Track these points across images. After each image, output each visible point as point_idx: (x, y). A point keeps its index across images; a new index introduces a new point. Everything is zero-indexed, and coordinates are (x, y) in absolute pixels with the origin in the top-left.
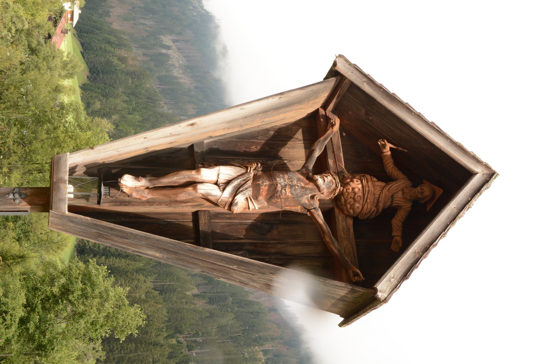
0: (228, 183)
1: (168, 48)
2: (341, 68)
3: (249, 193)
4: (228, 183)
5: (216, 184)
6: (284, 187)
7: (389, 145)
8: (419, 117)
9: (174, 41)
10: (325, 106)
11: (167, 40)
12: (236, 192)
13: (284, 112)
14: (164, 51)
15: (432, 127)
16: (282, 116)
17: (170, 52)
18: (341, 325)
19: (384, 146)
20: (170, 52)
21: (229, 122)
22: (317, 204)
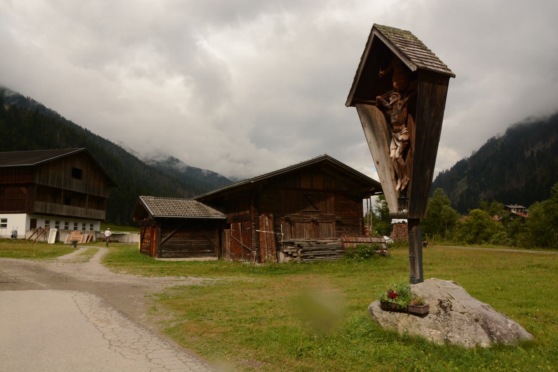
0: (396, 144)
1: (532, 152)
2: (348, 104)
3: (398, 134)
4: (396, 144)
5: (396, 149)
6: (394, 118)
7: (381, 72)
8: (360, 65)
9: (528, 150)
10: (373, 104)
11: (528, 154)
12: (398, 140)
13: (376, 121)
14: (535, 155)
15: (362, 59)
16: (379, 123)
17: (535, 151)
18: (454, 76)
19: (381, 74)
20: (535, 151)
21: (379, 146)
22: (402, 101)
